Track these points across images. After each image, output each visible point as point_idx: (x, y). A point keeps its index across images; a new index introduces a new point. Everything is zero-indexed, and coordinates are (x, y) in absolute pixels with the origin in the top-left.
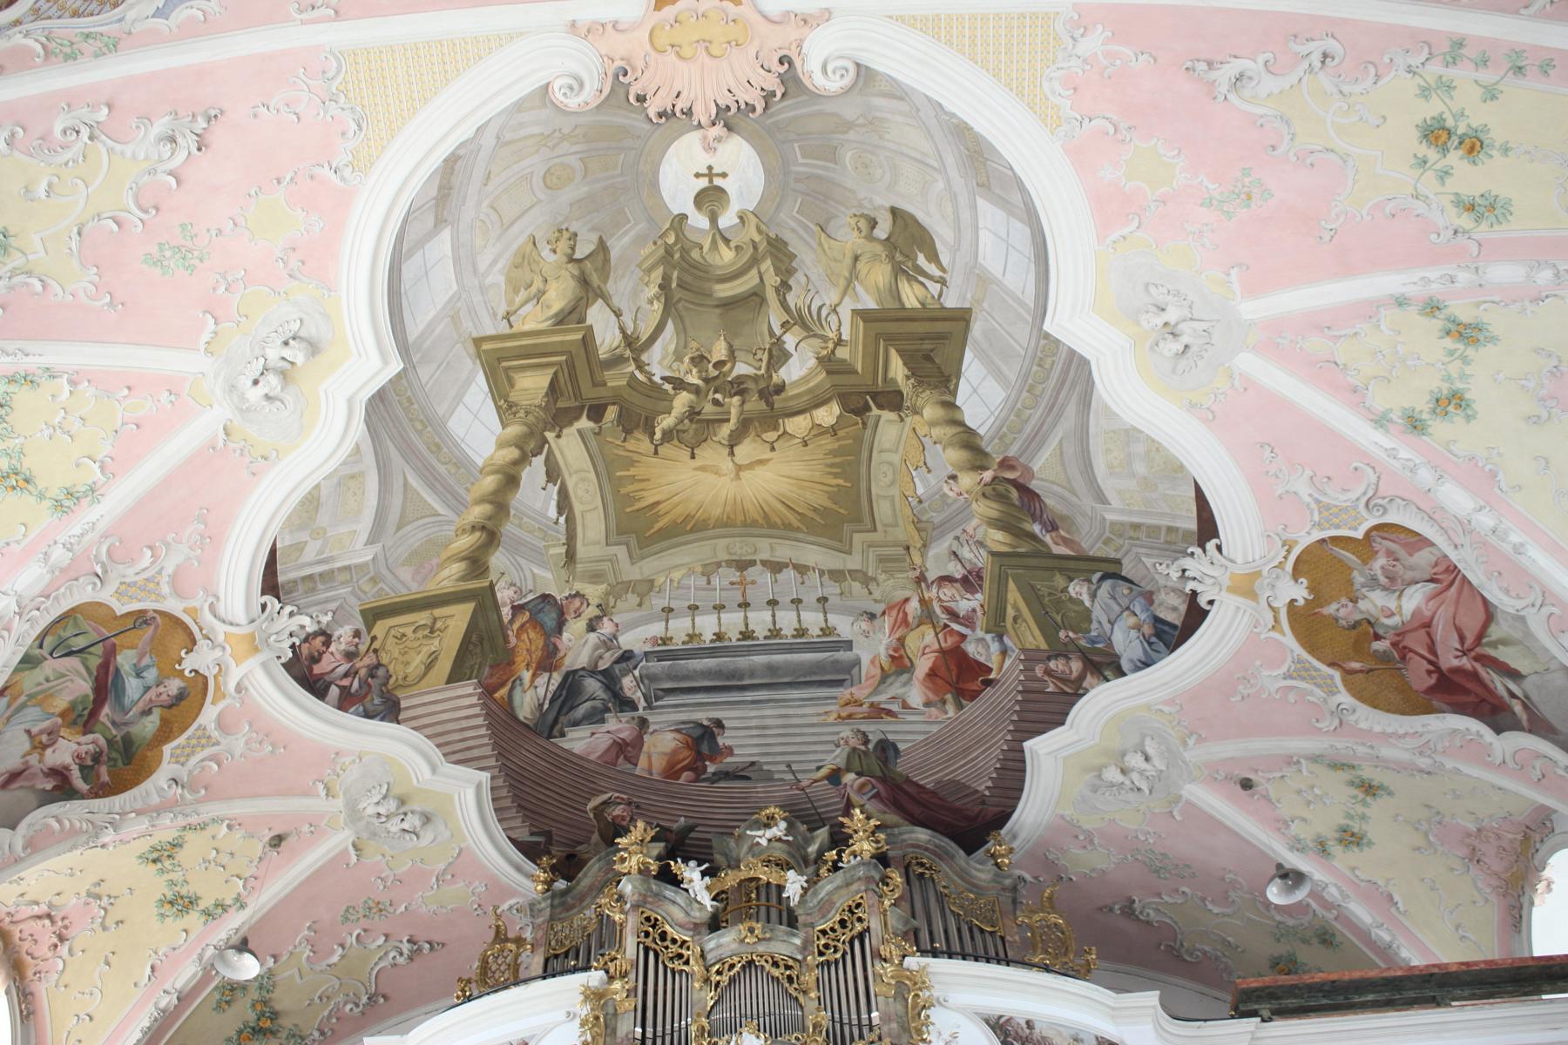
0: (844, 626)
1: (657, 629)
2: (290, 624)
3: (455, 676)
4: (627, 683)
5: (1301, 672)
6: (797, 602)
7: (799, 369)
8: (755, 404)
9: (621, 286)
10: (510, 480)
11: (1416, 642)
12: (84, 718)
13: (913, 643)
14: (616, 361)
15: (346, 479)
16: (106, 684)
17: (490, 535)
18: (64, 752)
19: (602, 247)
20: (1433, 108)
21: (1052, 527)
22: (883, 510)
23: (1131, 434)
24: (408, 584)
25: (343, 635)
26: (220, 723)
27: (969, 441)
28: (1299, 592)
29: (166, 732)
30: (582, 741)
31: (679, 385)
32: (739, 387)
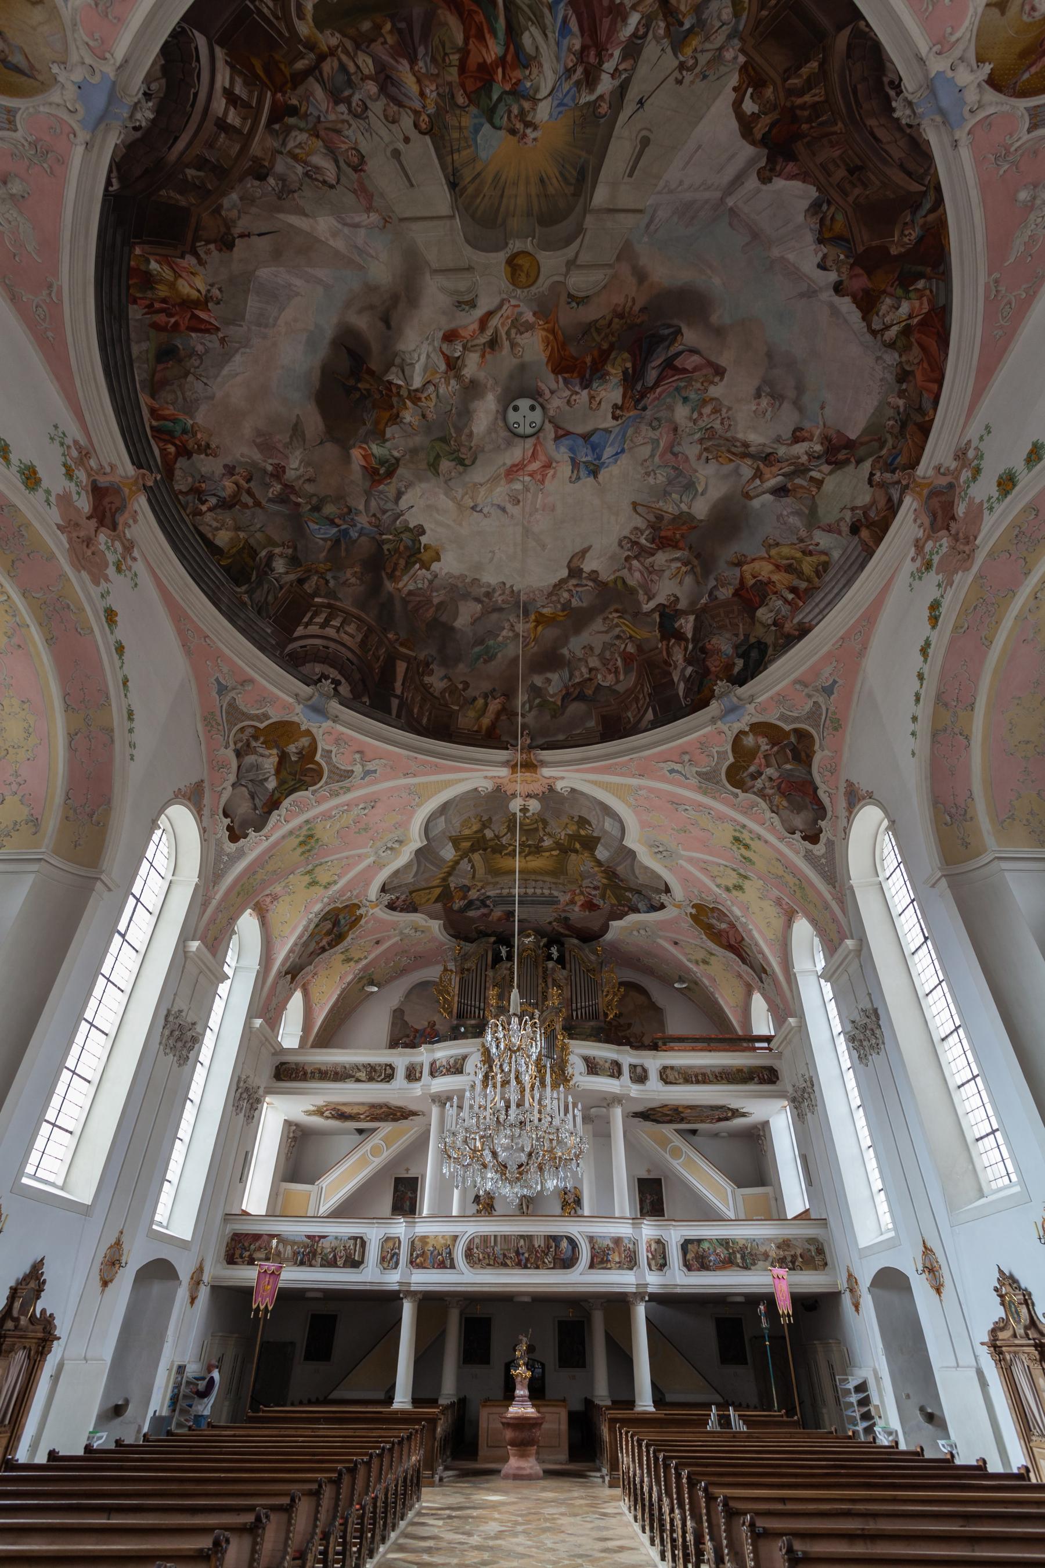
0: (556, 893)
1: (498, 891)
2: (387, 898)
3: (436, 901)
4: (488, 902)
5: (692, 926)
6: (542, 888)
7: (547, 842)
8: (533, 849)
9: (494, 826)
10: (457, 863)
11: (724, 934)
12: (329, 933)
13: (576, 898)
14: (492, 840)
15: (407, 866)
16: (336, 923)
17: (449, 874)
18: (324, 943)
19: (490, 819)
20: (737, 834)
21: (622, 881)
22: (570, 872)
23: (647, 868)
24: (424, 884)
25: (403, 897)
26: (366, 922)
27: (599, 863)
28: (694, 911)
29: (351, 928)
30: (471, 914)
31: (510, 845)
32: (529, 846)
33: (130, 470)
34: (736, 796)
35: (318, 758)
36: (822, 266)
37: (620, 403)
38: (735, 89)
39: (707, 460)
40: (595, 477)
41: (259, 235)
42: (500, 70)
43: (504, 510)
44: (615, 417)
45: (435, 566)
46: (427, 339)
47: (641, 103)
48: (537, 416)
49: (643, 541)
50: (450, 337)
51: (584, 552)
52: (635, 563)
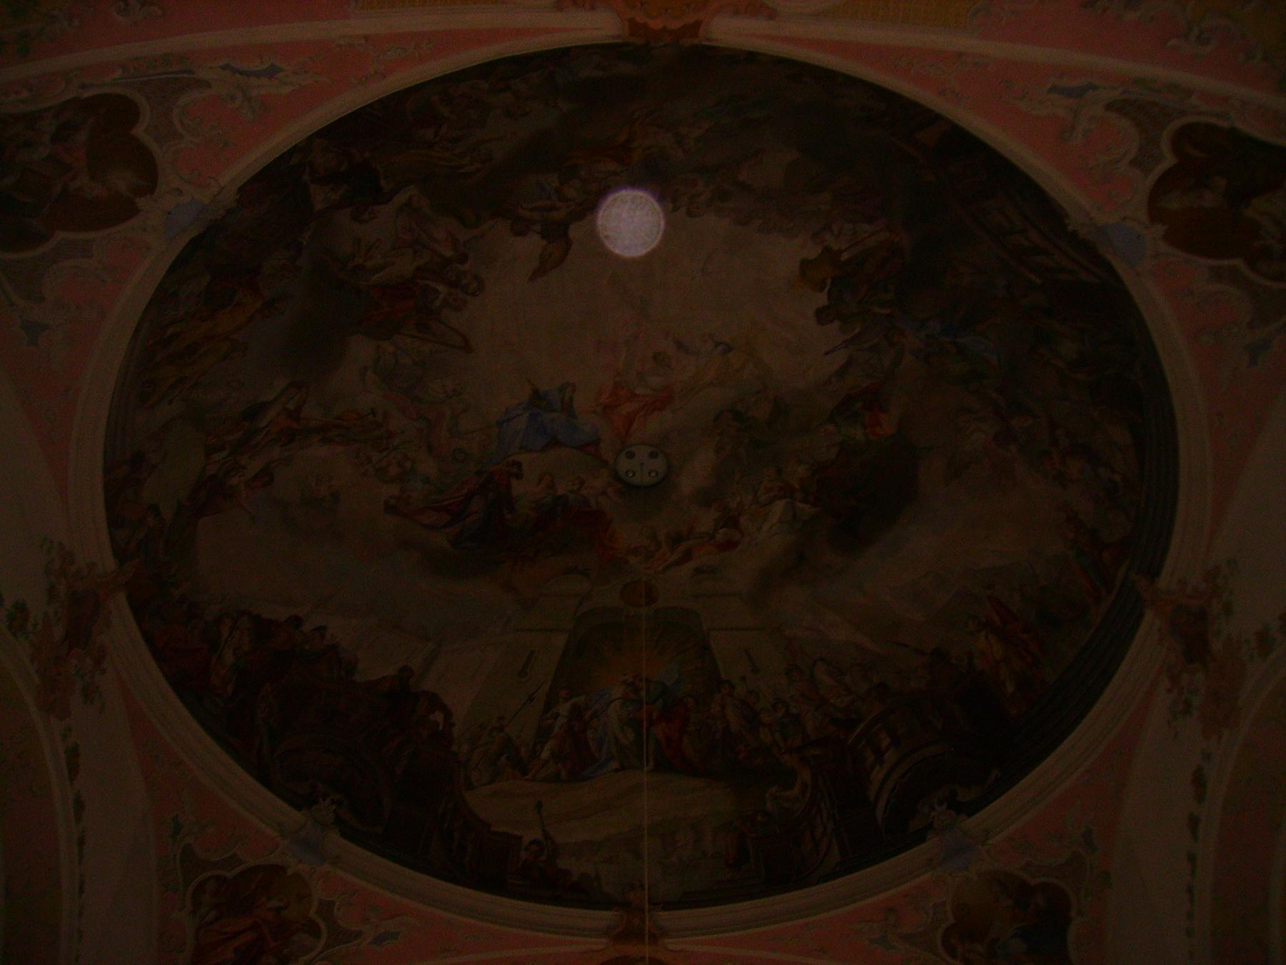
33: (1149, 615)
34: (84, 87)
35: (1169, 160)
36: (321, 630)
37: (514, 482)
38: (454, 725)
39: (373, 413)
40: (536, 391)
41: (906, 646)
42: (654, 717)
43: (680, 346)
44: (519, 465)
45: (813, 252)
46: (756, 544)
47: (531, 699)
48: (624, 464)
49: (442, 289)
50: (730, 545)
51: (542, 269)
52: (448, 253)
